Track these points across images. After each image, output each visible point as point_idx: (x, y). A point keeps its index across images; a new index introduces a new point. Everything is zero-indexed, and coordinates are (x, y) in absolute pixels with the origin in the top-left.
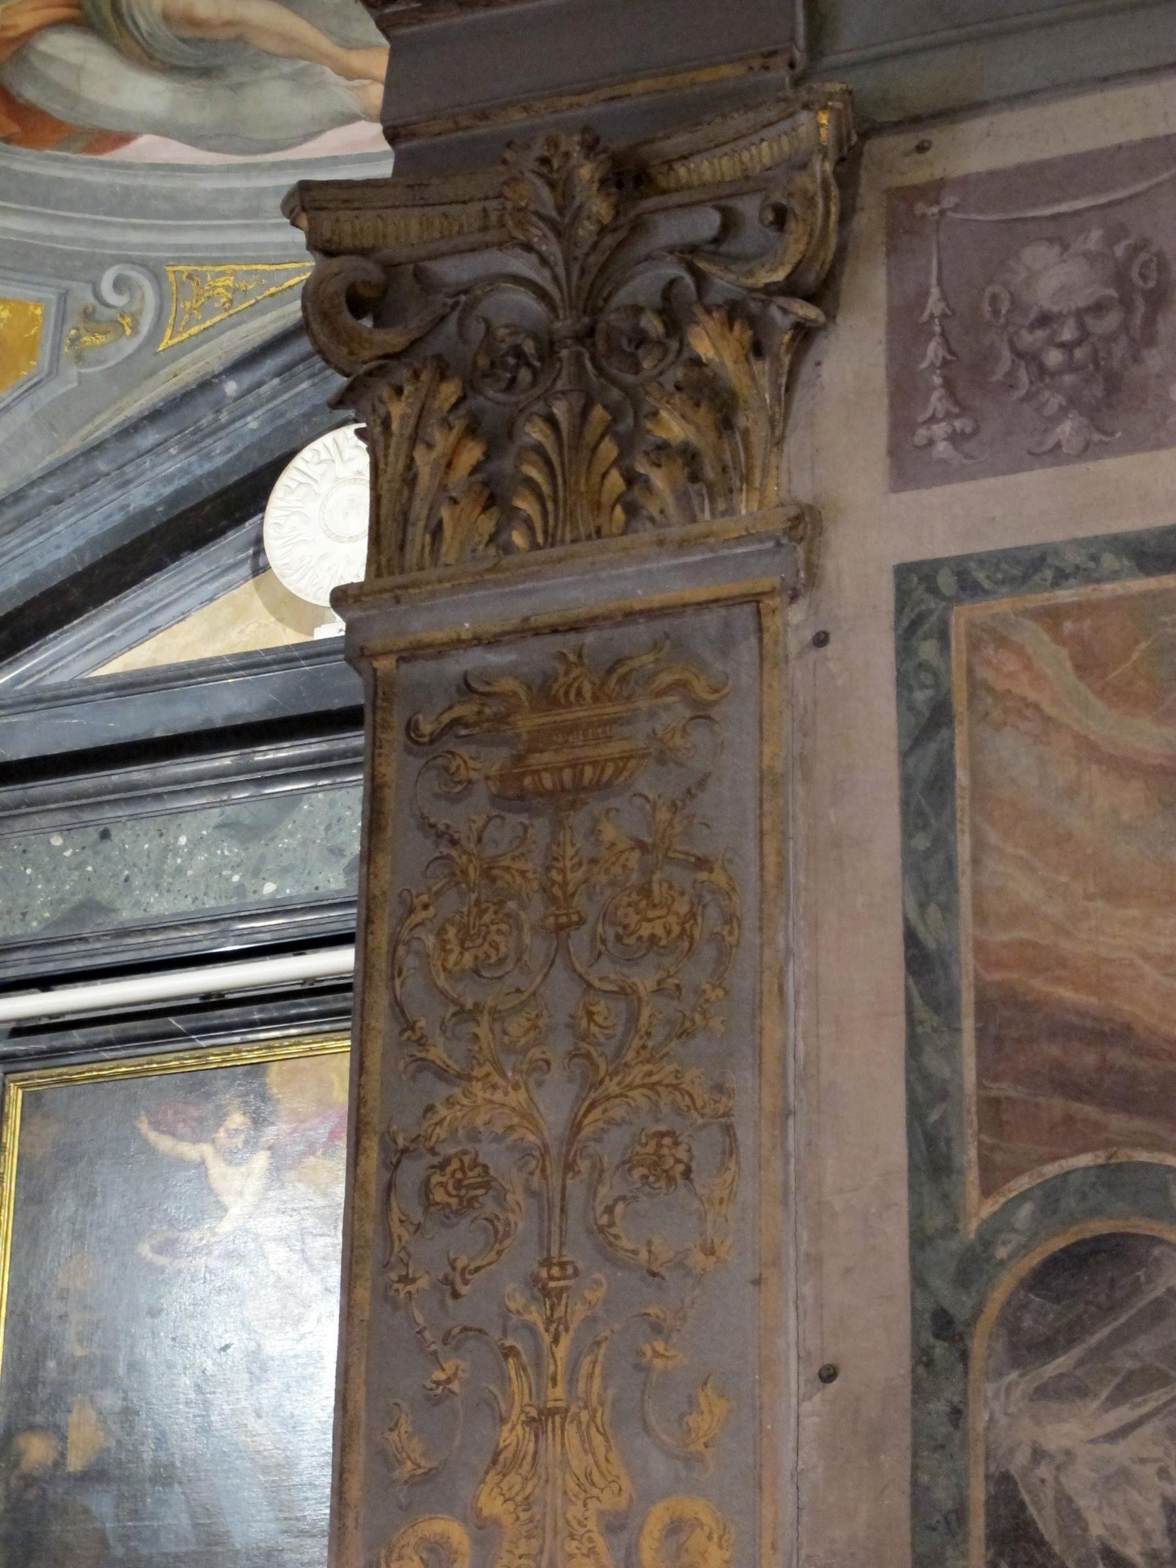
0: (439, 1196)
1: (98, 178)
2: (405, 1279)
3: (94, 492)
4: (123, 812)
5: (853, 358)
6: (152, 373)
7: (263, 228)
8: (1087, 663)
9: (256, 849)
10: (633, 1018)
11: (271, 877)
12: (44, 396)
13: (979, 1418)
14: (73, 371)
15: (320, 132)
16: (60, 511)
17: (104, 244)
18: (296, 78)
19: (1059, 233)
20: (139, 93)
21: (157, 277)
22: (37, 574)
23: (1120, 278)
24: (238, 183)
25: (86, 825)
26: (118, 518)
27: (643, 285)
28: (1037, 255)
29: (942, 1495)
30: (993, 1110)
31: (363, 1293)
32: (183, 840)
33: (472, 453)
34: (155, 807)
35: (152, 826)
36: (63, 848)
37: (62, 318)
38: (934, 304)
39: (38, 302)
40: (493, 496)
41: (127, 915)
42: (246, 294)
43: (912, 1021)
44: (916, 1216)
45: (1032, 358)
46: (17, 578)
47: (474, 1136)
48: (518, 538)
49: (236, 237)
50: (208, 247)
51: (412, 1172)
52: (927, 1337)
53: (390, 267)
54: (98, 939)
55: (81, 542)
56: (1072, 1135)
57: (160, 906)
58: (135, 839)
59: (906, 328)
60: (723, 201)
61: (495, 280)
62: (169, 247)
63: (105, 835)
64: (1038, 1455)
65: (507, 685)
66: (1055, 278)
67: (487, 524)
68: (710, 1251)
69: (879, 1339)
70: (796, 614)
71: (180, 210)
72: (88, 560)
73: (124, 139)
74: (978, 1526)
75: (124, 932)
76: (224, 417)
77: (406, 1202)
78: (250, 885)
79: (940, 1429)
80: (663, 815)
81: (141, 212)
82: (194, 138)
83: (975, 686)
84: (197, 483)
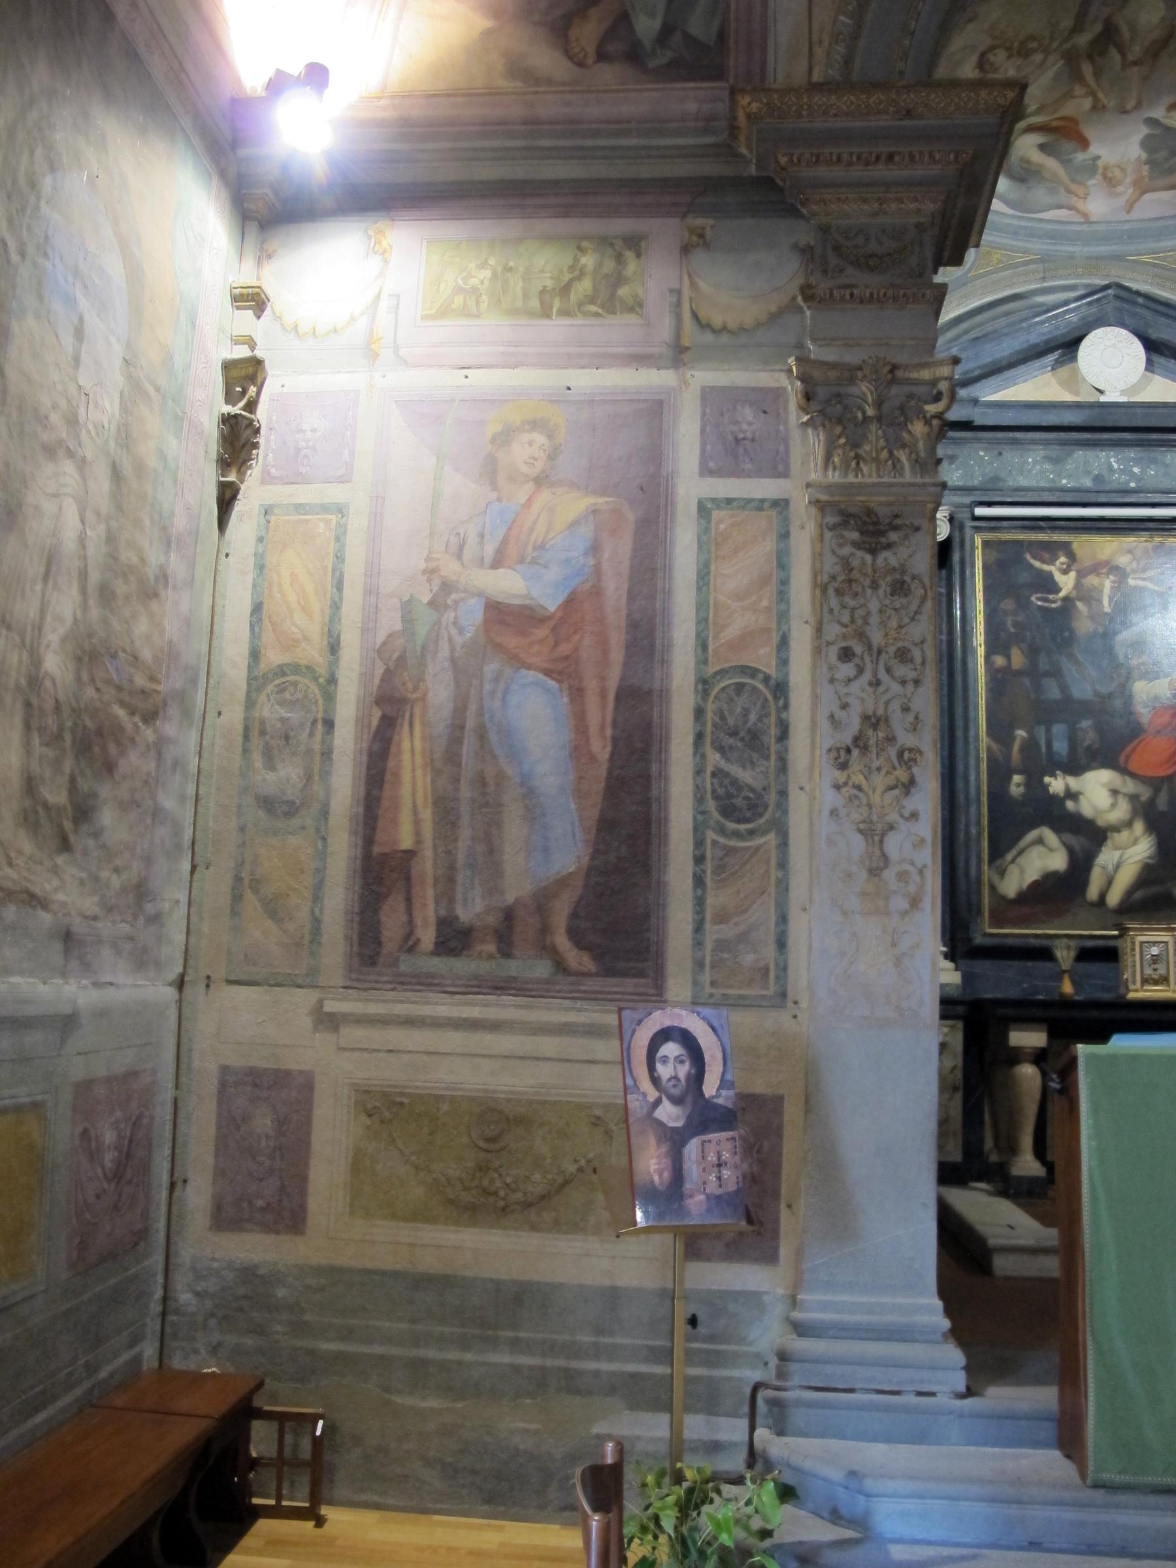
6: (965, 284)
24: (1016, 222)
26: (1025, 345)
41: (1011, 483)
57: (1023, 482)
58: (1012, 457)
63: (1000, 454)
75: (1017, 489)
84: (1055, 338)
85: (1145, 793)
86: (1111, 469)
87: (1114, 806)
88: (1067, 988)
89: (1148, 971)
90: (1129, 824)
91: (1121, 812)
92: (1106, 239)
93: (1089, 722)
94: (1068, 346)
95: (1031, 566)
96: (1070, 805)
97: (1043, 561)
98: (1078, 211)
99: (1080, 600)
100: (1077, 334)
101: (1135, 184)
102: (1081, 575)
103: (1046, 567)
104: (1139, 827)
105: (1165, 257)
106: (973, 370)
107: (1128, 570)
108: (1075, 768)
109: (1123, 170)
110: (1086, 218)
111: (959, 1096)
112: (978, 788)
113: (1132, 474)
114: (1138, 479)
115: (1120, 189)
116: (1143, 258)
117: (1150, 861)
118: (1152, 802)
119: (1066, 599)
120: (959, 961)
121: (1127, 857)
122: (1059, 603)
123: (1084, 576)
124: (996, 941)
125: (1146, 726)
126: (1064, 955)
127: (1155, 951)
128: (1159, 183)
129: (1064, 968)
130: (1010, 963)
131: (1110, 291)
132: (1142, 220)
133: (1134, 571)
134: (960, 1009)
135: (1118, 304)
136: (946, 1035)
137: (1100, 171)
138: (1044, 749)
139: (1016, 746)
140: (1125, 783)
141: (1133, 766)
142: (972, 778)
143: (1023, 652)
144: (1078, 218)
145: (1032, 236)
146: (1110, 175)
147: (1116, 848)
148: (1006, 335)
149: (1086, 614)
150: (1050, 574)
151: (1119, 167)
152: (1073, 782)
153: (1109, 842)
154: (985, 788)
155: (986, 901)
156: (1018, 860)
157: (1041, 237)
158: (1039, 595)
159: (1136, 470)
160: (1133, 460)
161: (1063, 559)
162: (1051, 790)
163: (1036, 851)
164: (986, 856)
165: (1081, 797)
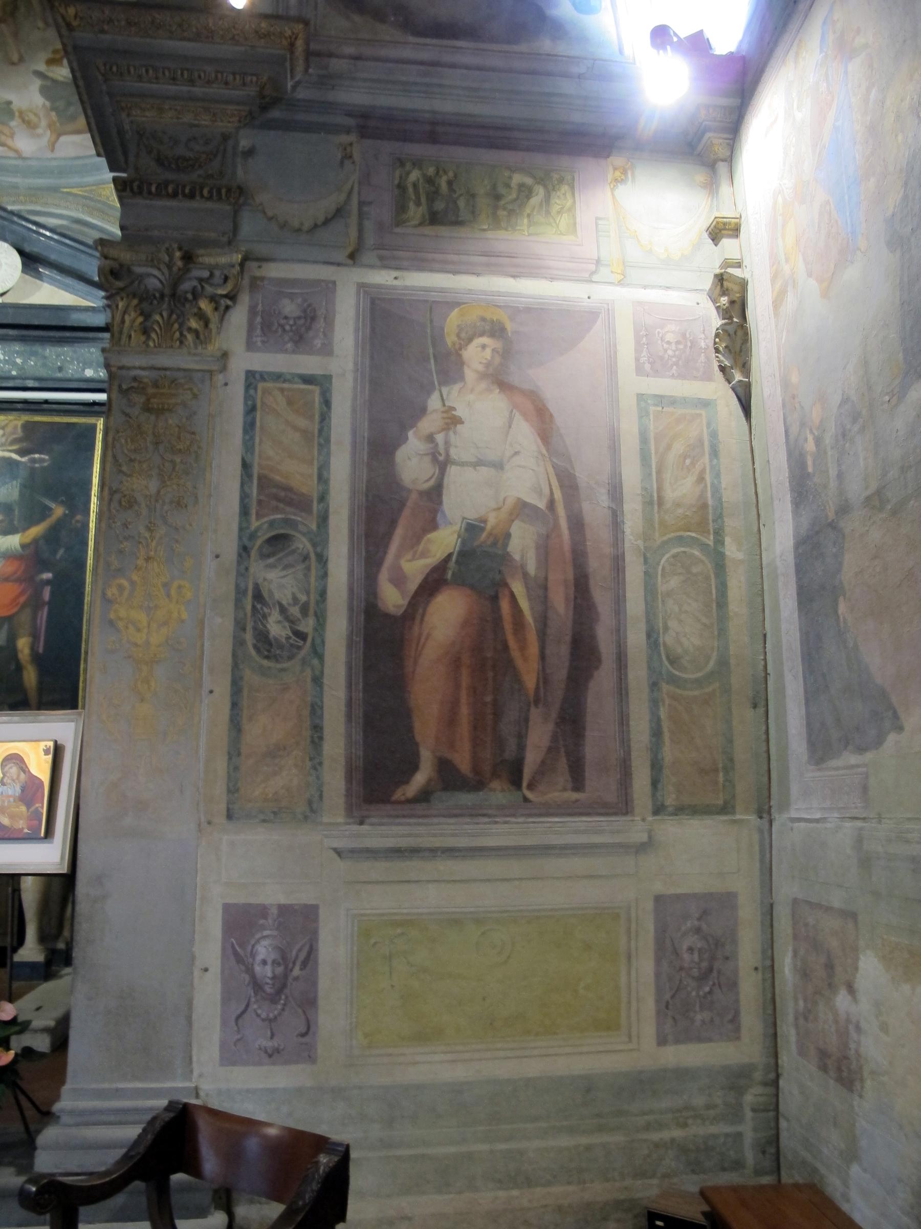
0: (123, 503)
2: (114, 522)
5: (239, 316)
8: (290, 403)
10: (174, 469)
13: (252, 570)
19: (292, 297)
23: (305, 311)
27: (186, 286)
28: (286, 301)
29: (242, 585)
30: (260, 502)
31: (103, 525)
33: (140, 319)
38: (260, 307)
40: (146, 331)
43: (242, 479)
44: (240, 523)
45: (282, 326)
47: (133, 490)
48: (151, 344)
51: (117, 497)
52: (241, 551)
53: (121, 265)
56: (276, 510)
59: (253, 312)
60: (211, 269)
61: (149, 275)
64: (265, 579)
65: (146, 380)
66: (289, 308)
67: (143, 338)
68: (191, 525)
69: (230, 549)
70: (221, 377)
74: (250, 593)
77: (115, 504)
79: (242, 572)
80: (184, 420)
83: (263, 403)
92: (40, 173)
98: (9, 148)
101: (50, 126)
105: (91, 191)
109: (36, 115)
110: (19, 155)
113: (15, 363)
114: (20, 368)
115: (39, 131)
116: (75, 191)
132: (64, 159)
137: (17, 114)
144: (12, 154)
146: (26, 118)
159: (19, 361)
160: (17, 352)
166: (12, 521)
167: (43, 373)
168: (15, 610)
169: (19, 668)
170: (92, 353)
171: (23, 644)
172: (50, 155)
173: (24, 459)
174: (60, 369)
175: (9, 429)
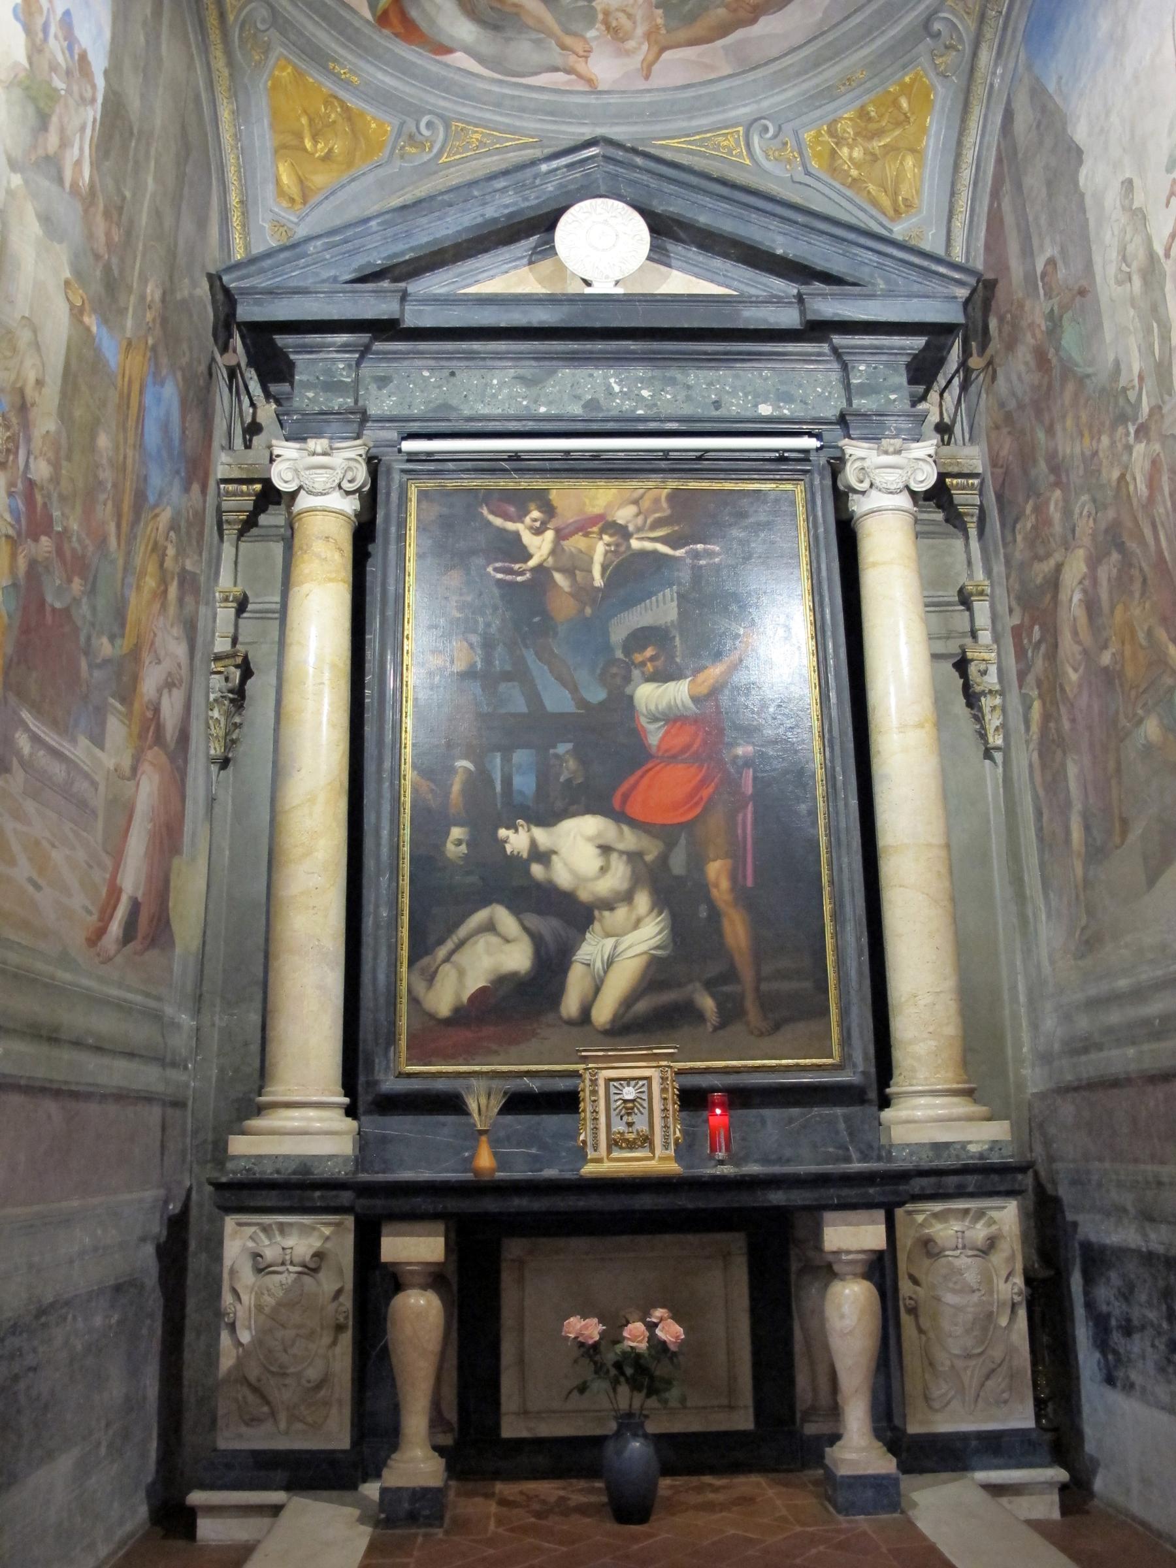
1: (434, 68)
3: (469, 205)
4: (463, 364)
6: (436, 173)
7: (501, 114)
9: (535, 391)
11: (543, 405)
12: (382, 172)
14: (398, 163)
15: (540, 73)
16: (452, 210)
17: (427, 103)
18: (537, 42)
20: (464, 30)
21: (447, 127)
22: (435, 241)
24: (496, 89)
25: (442, 368)
26: (480, 220)
32: (495, 382)
34: (481, 363)
35: (478, 373)
36: (430, 377)
37: (399, 135)
39: (390, 124)
41: (467, 412)
42: (485, 145)
46: (425, 240)
49: (488, 116)
50: (474, 117)
54: (457, 421)
55: (460, 228)
57: (483, 409)
58: (469, 377)
62: (455, 112)
63: (453, 374)
71: (466, 95)
72: (464, 237)
73: (449, 51)
75: (470, 419)
76: (538, 182)
78: (533, 407)
81: (447, 91)
82: (481, 60)
85: (652, 850)
86: (610, 392)
87: (604, 870)
88: (485, 1159)
89: (619, 1127)
90: (627, 897)
91: (617, 877)
93: (570, 746)
94: (538, 227)
95: (489, 523)
96: (537, 870)
97: (507, 517)
98: (580, 76)
99: (558, 570)
100: (554, 206)
102: (560, 535)
103: (510, 526)
104: (643, 901)
106: (403, 253)
107: (631, 528)
108: (548, 818)
109: (630, 16)
110: (592, 87)
111: (347, 1338)
112: (396, 849)
115: (631, 44)
117: (659, 953)
118: (664, 859)
119: (540, 569)
120: (363, 1118)
121: (623, 950)
122: (528, 575)
123: (565, 538)
124: (416, 1085)
125: (654, 750)
126: (482, 1105)
127: (629, 1093)
128: (683, 35)
129: (479, 1127)
130: (442, 1118)
131: (593, 151)
132: (664, 90)
133: (639, 529)
134: (346, 1197)
135: (611, 168)
136: (327, 1239)
137: (600, 17)
138: (498, 788)
139: (456, 788)
140: (621, 832)
141: (635, 810)
142: (385, 833)
143: (471, 646)
144: (582, 86)
145: (523, 110)
146: (614, 24)
147: (608, 935)
148: (451, 205)
149: (567, 589)
150: (517, 536)
151: (624, 11)
152: (540, 834)
153: (597, 926)
154: (406, 849)
155: (403, 1023)
156: (455, 958)
157: (535, 112)
158: (498, 565)
159: (645, 393)
161: (535, 514)
162: (509, 848)
163: (482, 943)
164: (404, 953)
165: (554, 858)
166: (671, 658)
167: (687, 410)
168: (698, 810)
169: (715, 915)
170: (766, 379)
171: (716, 870)
172: (642, 85)
173: (680, 553)
174: (717, 404)
175: (646, 504)
